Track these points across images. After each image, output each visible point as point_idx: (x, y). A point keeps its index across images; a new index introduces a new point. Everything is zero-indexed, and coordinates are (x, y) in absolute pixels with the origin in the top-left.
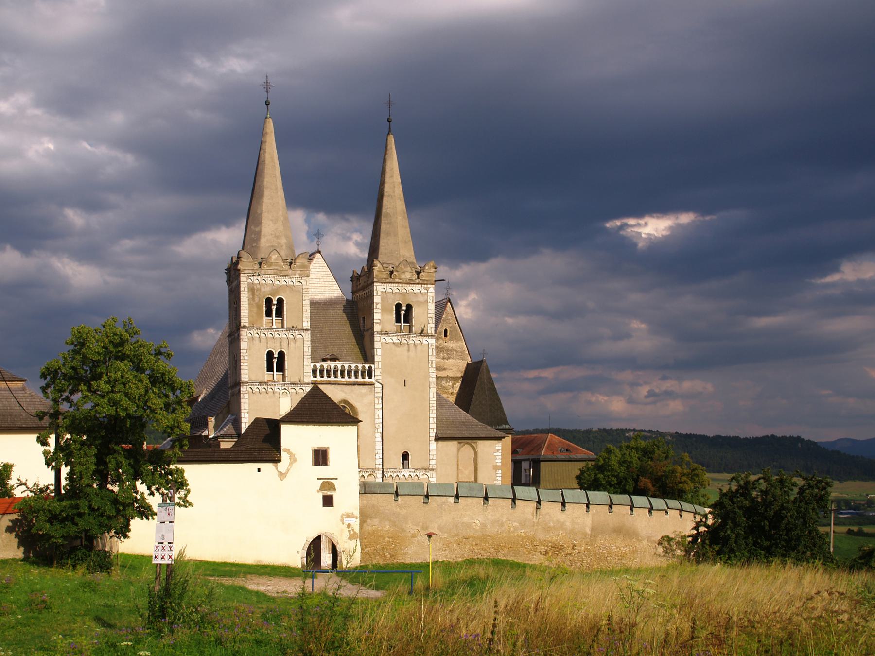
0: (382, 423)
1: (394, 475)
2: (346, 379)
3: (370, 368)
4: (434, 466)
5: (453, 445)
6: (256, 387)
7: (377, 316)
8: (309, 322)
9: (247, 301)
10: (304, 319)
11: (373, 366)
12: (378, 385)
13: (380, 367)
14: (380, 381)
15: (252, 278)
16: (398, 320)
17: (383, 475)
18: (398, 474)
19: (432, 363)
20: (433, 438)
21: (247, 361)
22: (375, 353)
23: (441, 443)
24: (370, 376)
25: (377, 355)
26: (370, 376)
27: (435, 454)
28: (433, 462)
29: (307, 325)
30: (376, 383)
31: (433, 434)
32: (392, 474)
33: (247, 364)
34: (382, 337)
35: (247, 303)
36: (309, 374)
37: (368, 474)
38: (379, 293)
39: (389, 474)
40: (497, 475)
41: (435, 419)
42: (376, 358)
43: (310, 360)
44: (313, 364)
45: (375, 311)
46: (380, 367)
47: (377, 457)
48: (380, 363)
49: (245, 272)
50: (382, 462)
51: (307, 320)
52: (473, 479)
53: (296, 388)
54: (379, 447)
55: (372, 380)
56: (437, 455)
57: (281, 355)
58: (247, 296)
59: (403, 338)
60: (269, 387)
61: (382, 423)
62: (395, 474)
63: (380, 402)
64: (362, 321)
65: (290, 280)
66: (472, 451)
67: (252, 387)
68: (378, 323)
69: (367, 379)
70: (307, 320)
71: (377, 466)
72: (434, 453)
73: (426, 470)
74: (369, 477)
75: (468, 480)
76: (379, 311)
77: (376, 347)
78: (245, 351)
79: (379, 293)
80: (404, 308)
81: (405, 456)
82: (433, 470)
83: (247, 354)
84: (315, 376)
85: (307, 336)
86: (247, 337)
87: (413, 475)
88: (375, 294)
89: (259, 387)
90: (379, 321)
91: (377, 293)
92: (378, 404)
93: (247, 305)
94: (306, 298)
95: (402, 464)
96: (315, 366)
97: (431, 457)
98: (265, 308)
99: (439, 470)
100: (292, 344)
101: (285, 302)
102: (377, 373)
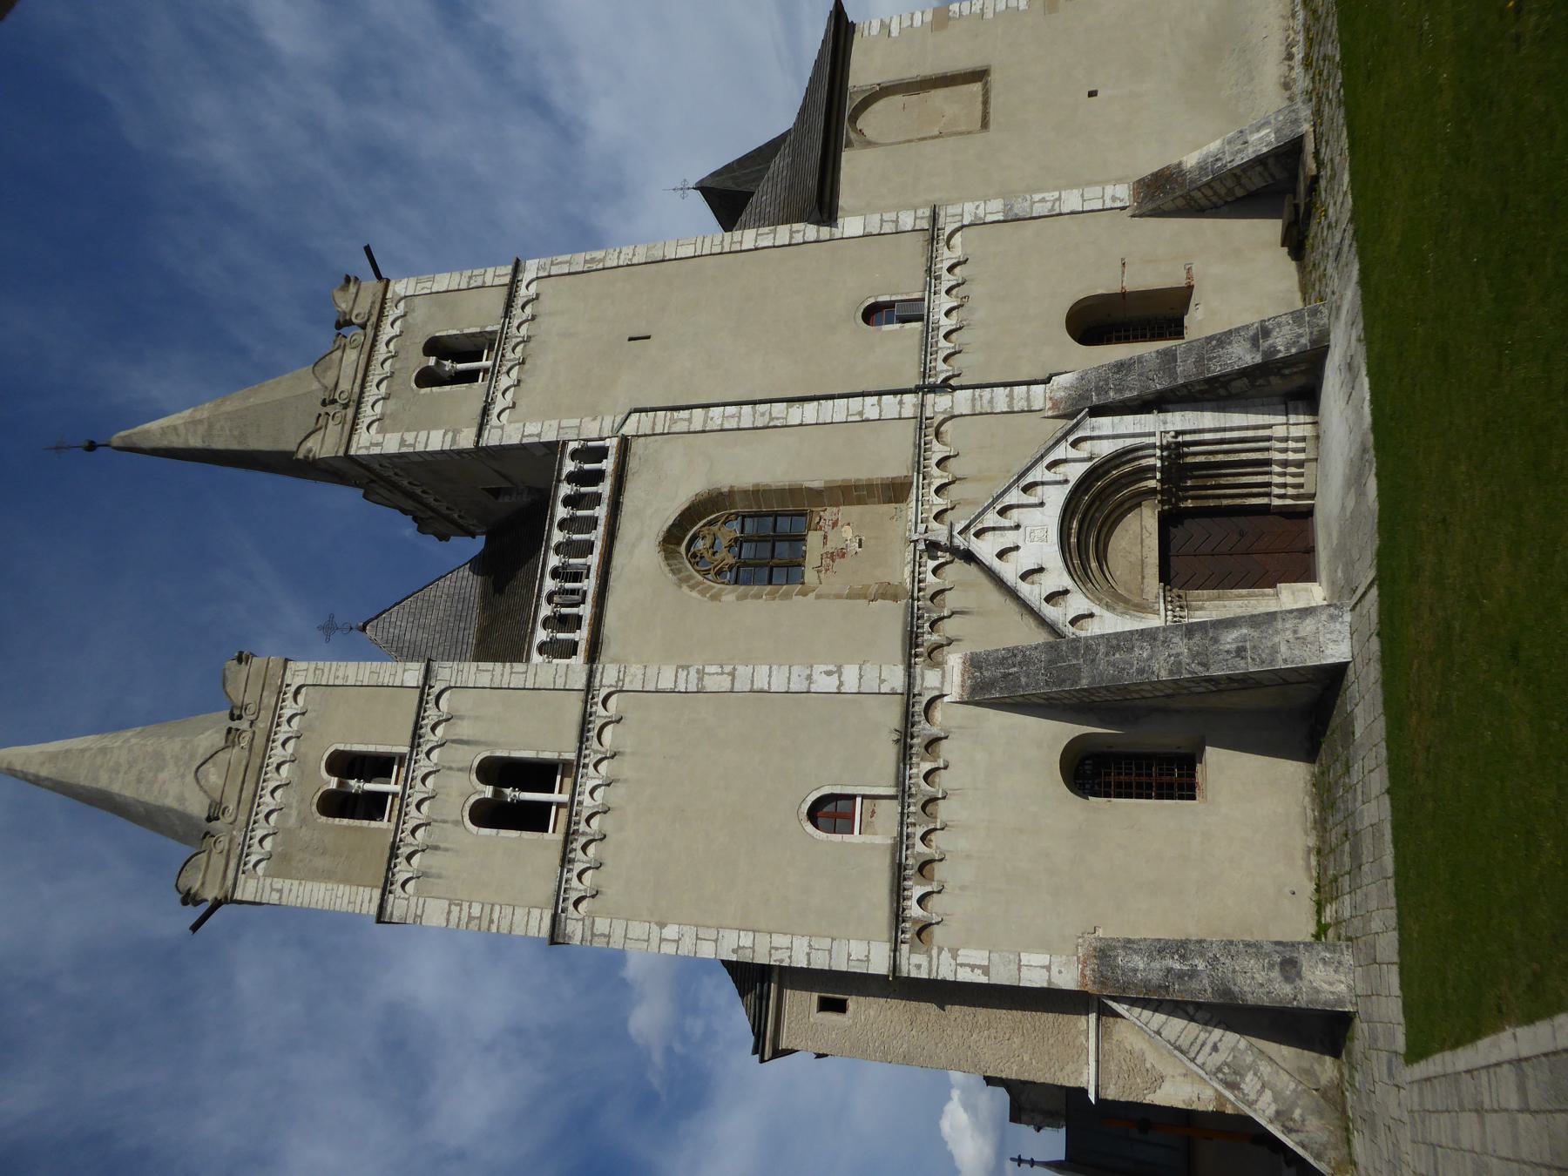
0: (754, 403)
1: (945, 347)
2: (598, 536)
3: (575, 455)
4: (920, 213)
5: (852, 164)
6: (575, 883)
7: (435, 441)
8: (409, 665)
9: (309, 885)
10: (398, 683)
11: (572, 446)
12: (628, 429)
13: (576, 422)
14: (619, 420)
15: (253, 859)
16: (470, 377)
17: (946, 386)
18: (942, 332)
19: (593, 260)
20: (825, 232)
21: (487, 909)
22: (536, 440)
23: (844, 200)
24: (601, 454)
25: (539, 435)
26: (601, 454)
27: (877, 217)
28: (907, 220)
29: (412, 674)
30: (622, 431)
31: (811, 231)
32: (941, 355)
33: (497, 908)
34: (494, 420)
35: (316, 885)
36: (562, 671)
37: (936, 446)
38: (379, 438)
39: (941, 366)
40: (966, 12)
41: (761, 230)
42: (550, 436)
43: (519, 667)
44: (536, 657)
45: (420, 448)
46: (576, 422)
47: (872, 413)
48: (565, 423)
49: (229, 882)
50: (895, 393)
51: (400, 671)
52: (976, 87)
53: (599, 723)
54: (837, 410)
55: (612, 443)
56: (882, 210)
57: (497, 771)
58: (296, 883)
59: (509, 355)
60: (582, 827)
61: (754, 403)
62: (943, 343)
63: (684, 414)
64: (507, 499)
65: (285, 727)
66: (878, 106)
67: (574, 896)
68: (454, 439)
69: (608, 465)
70: (400, 671)
71: (909, 411)
72: (877, 217)
73: (933, 240)
74: (948, 438)
75: (980, 99)
76: (423, 435)
77: (515, 440)
78: (455, 909)
79: (379, 438)
80: (432, 361)
81: (873, 314)
82: (934, 217)
83: (465, 906)
84: (570, 649)
85: (446, 672)
86: (413, 900)
87: (947, 280)
88: (376, 451)
89: (578, 867)
90: (450, 435)
91: (377, 445)
92: (690, 420)
93: (323, 886)
94: (340, 674)
95: (908, 326)
96: (542, 648)
97: (888, 228)
98: (345, 821)
99: (935, 197)
100: (464, 729)
101: (341, 747)
102: (594, 429)
